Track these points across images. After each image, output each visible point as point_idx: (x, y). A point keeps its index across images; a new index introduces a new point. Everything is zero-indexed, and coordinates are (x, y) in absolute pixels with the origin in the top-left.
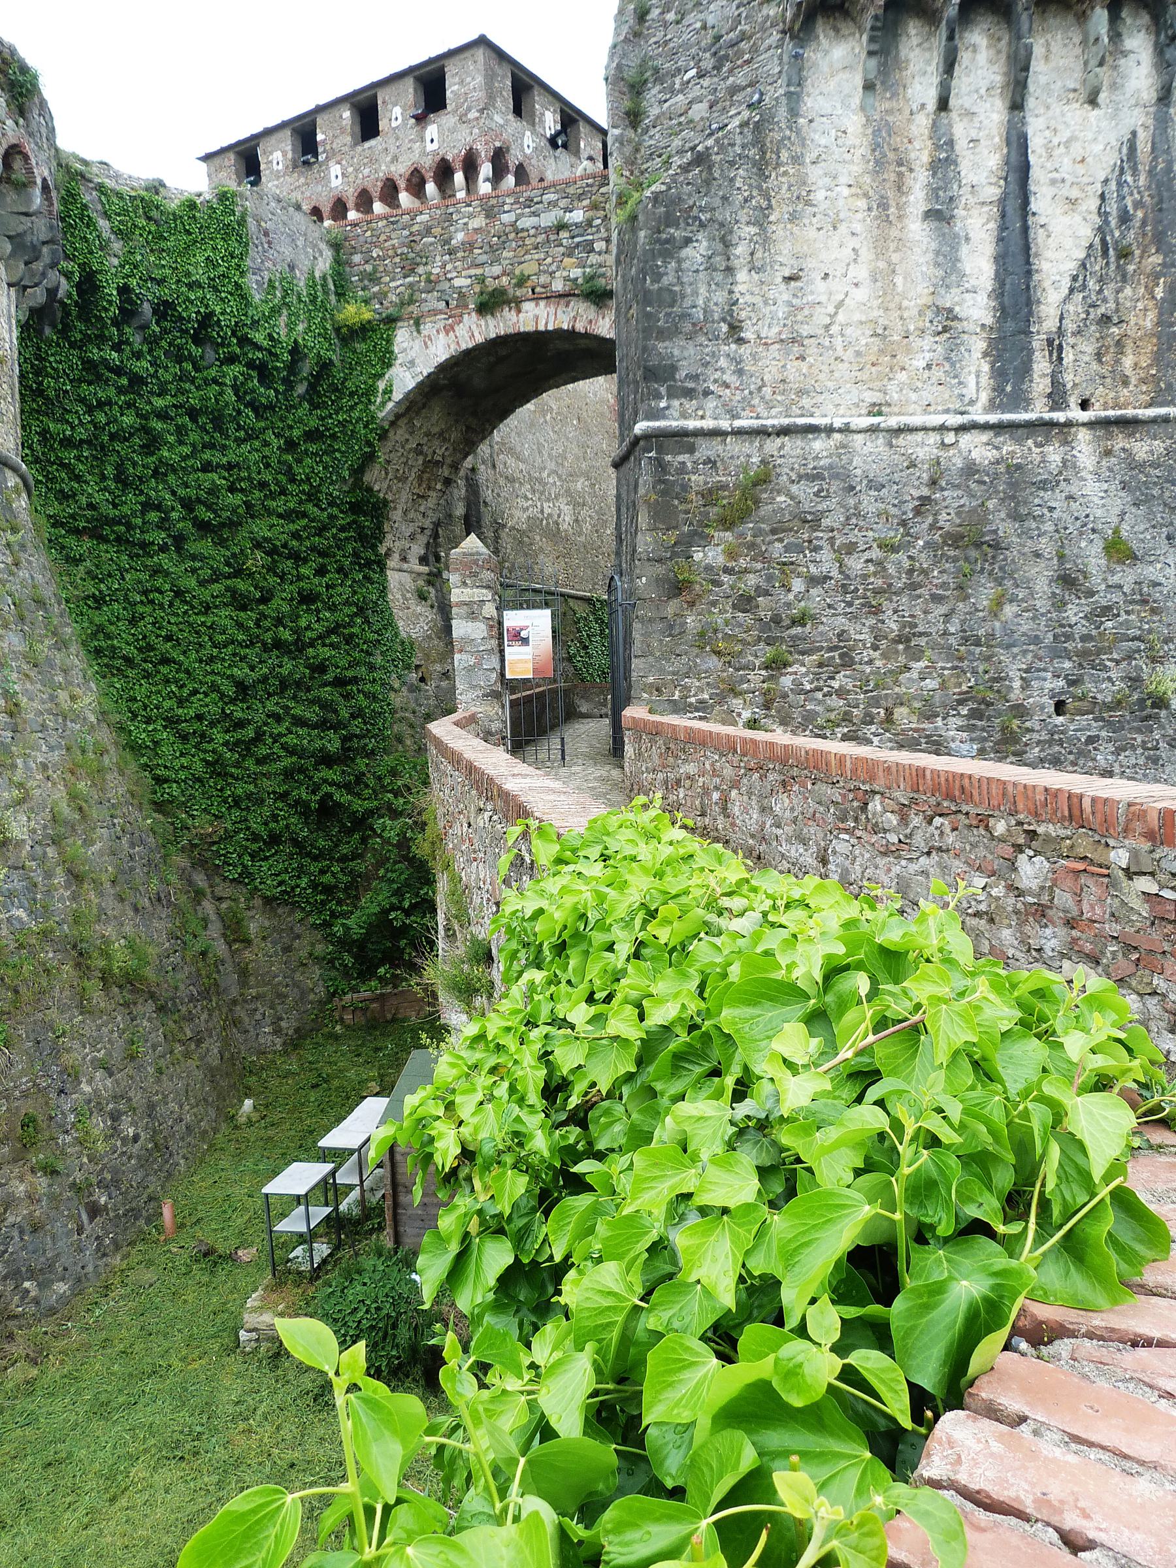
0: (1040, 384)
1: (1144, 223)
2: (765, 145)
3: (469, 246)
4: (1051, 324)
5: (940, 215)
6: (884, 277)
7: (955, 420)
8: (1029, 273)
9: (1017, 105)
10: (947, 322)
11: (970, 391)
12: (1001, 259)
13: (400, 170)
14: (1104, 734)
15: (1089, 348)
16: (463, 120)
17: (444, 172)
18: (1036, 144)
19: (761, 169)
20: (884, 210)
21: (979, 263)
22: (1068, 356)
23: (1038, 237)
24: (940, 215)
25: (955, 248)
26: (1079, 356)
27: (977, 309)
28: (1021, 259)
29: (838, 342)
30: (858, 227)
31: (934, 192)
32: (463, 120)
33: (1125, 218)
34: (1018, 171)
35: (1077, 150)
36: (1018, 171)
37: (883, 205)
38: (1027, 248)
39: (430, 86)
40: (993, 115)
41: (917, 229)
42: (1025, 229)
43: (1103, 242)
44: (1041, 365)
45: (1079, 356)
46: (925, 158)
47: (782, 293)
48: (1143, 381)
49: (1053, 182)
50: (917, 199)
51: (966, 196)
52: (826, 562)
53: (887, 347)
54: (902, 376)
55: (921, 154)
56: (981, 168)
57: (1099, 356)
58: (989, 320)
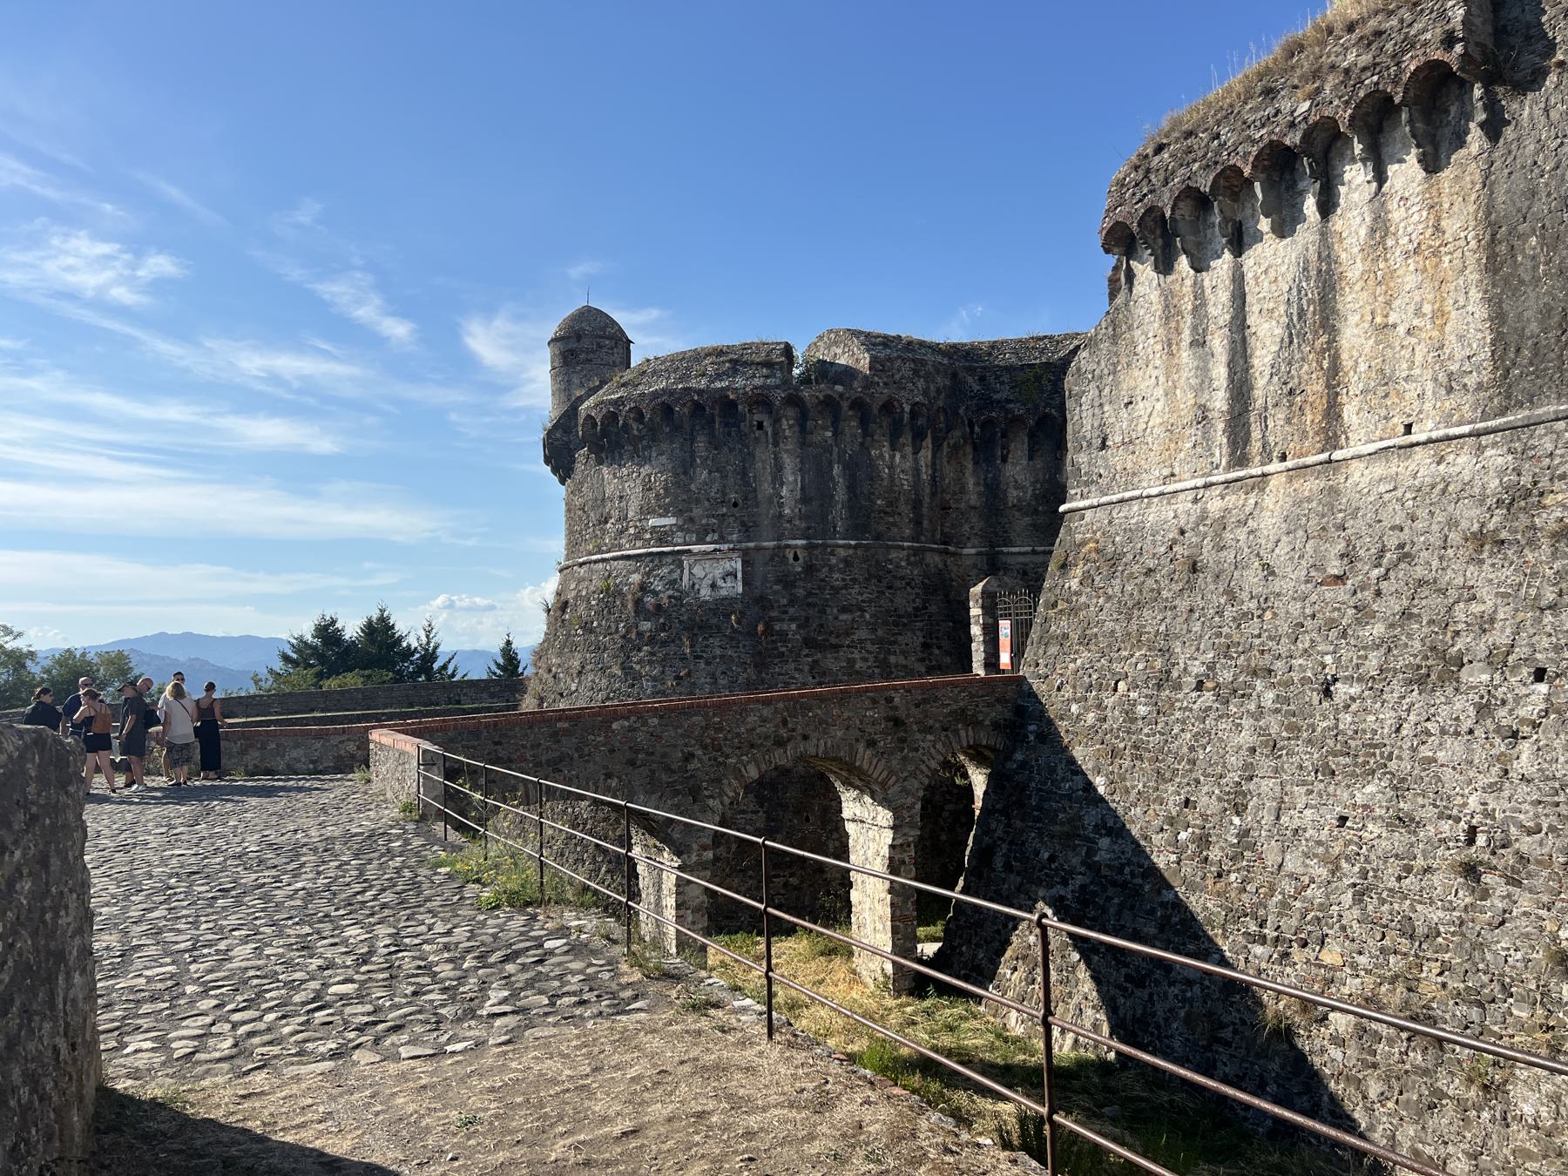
0: (1255, 446)
1: (1314, 313)
2: (1117, 326)
4: (1260, 402)
5: (1199, 343)
7: (1200, 482)
8: (1247, 367)
11: (1216, 460)
12: (1231, 365)
14: (1216, 705)
15: (1281, 415)
18: (1249, 276)
19: (1115, 339)
21: (1220, 372)
22: (1271, 424)
23: (1252, 341)
24: (1199, 343)
25: (1206, 362)
26: (1277, 419)
27: (1219, 401)
28: (1241, 362)
29: (1150, 440)
30: (1158, 363)
31: (1194, 328)
33: (1301, 314)
35: (1272, 274)
37: (1170, 345)
38: (1245, 350)
41: (1185, 356)
42: (1244, 340)
43: (1291, 335)
44: (1256, 434)
45: (1277, 419)
46: (1190, 307)
47: (1124, 413)
48: (1317, 433)
49: (1259, 300)
50: (1186, 336)
51: (1212, 327)
54: (1182, 455)
55: (1187, 305)
57: (1288, 421)
58: (1225, 408)
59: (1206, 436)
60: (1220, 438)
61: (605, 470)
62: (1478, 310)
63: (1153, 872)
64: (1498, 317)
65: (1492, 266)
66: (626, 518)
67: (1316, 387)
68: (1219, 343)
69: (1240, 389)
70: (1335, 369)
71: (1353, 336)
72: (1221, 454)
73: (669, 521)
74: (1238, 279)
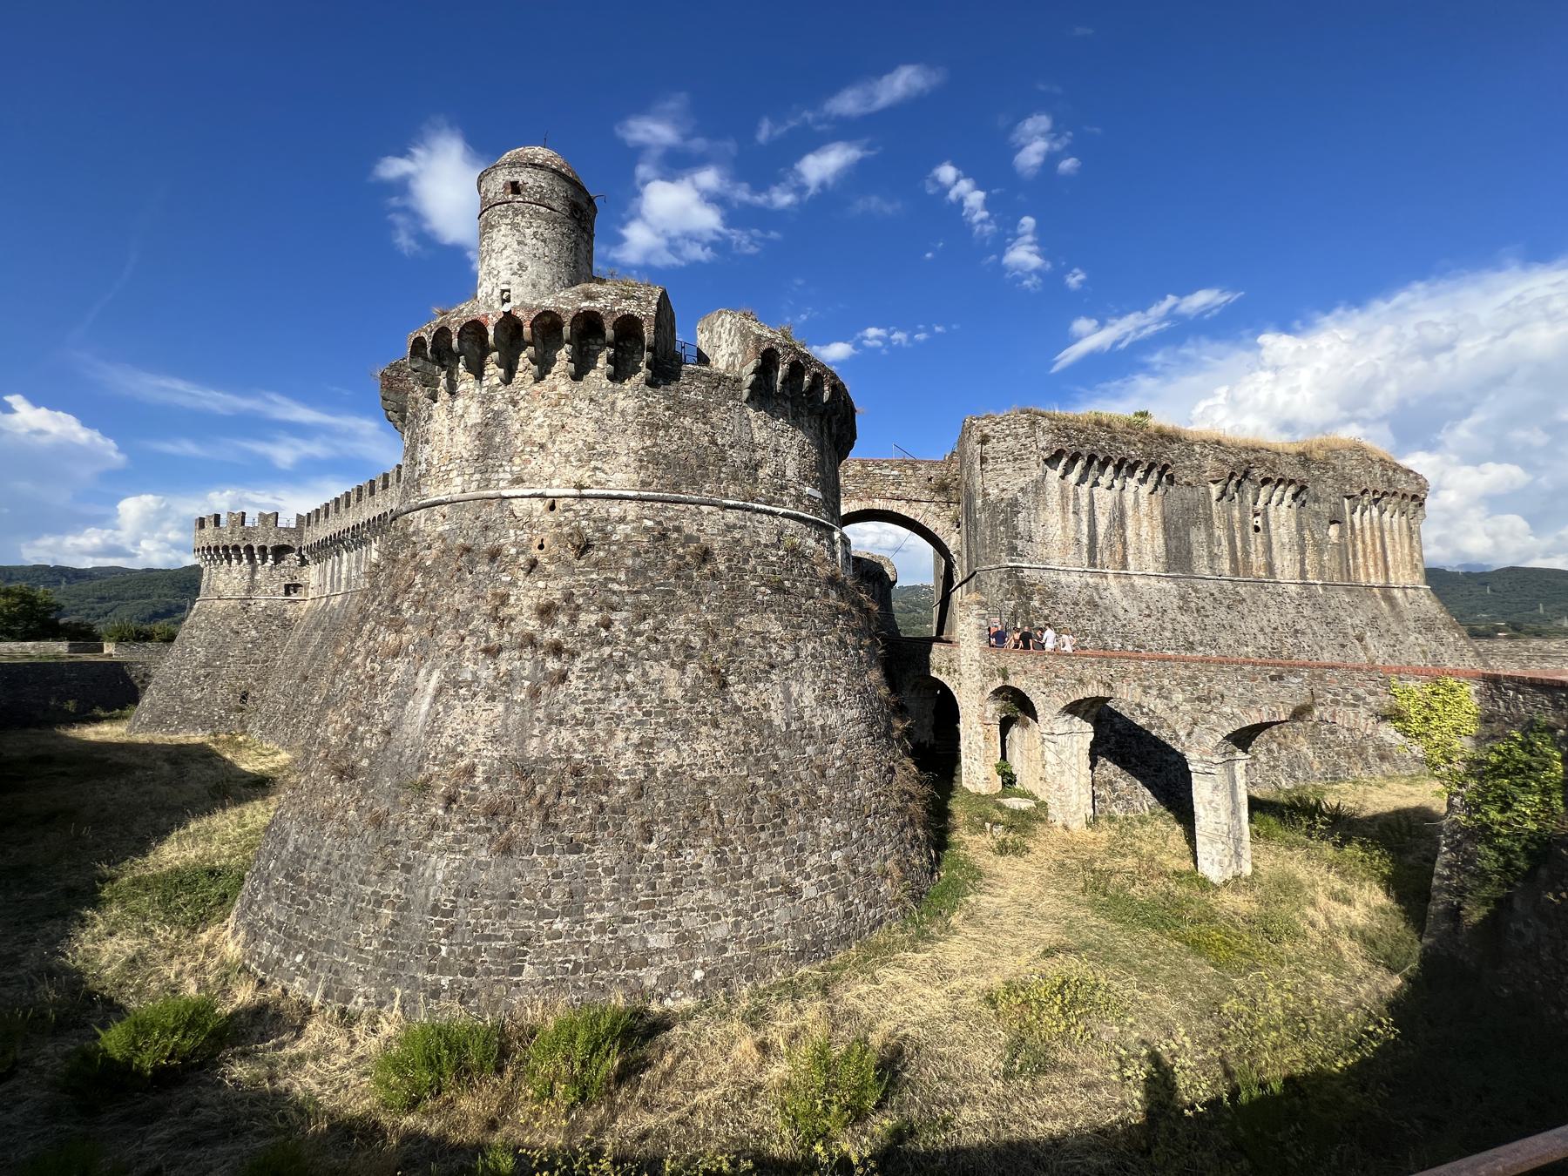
3: (855, 476)
6: (1064, 528)
20: (1064, 509)
21: (1085, 528)
27: (1085, 540)
34: (1092, 503)
36: (1092, 503)
41: (1071, 516)
45: (1107, 553)
52: (1061, 608)
53: (1065, 546)
56: (1084, 501)
59: (1080, 550)
61: (750, 412)
62: (1160, 541)
63: (1140, 728)
64: (1166, 544)
65: (1165, 530)
66: (784, 476)
67: (1118, 547)
68: (1084, 517)
69: (1093, 537)
70: (1124, 543)
71: (1130, 534)
72: (1085, 561)
73: (818, 494)
74: (1091, 496)
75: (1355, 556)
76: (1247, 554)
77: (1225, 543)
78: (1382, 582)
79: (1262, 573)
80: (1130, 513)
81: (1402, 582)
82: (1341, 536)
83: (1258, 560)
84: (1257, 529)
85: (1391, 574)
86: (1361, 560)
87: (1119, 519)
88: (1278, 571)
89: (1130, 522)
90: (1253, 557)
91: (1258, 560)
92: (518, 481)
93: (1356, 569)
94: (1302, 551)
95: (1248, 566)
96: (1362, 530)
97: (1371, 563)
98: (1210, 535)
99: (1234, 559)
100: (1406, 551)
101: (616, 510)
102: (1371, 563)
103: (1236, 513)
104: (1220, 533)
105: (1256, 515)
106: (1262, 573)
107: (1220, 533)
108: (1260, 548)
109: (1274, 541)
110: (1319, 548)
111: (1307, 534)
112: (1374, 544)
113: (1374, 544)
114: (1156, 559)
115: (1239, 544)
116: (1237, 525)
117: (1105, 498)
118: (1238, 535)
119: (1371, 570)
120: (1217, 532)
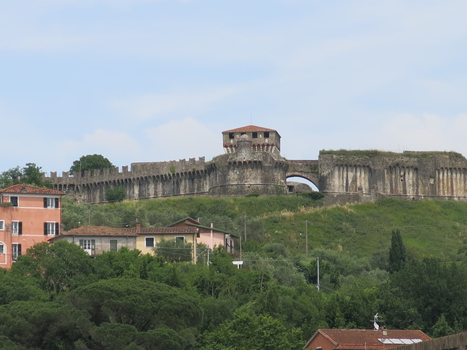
2: (332, 173)
5: (343, 179)
6: (339, 182)
9: (347, 172)
10: (343, 186)
13: (261, 143)
16: (272, 140)
17: (268, 145)
21: (345, 182)
24: (343, 179)
27: (345, 185)
32: (272, 140)
34: (347, 176)
36: (347, 176)
39: (266, 134)
40: (346, 172)
53: (339, 187)
56: (345, 176)
60: (345, 189)
67: (355, 186)
75: (439, 187)
76: (396, 187)
77: (389, 185)
78: (450, 195)
79: (401, 193)
80: (358, 178)
81: (459, 195)
82: (435, 182)
83: (400, 189)
84: (402, 180)
85: (455, 193)
86: (441, 188)
87: (355, 180)
88: (408, 192)
89: (358, 180)
90: (399, 188)
91: (400, 189)
92: (246, 182)
93: (439, 191)
94: (418, 186)
95: (396, 191)
96: (443, 179)
97: (446, 189)
98: (384, 183)
99: (392, 190)
100: (462, 185)
101: (259, 186)
102: (446, 189)
103: (394, 176)
104: (387, 182)
105: (401, 176)
106: (401, 193)
107: (387, 182)
108: (402, 186)
109: (407, 184)
110: (424, 186)
111: (420, 181)
112: (448, 183)
113: (448, 183)
114: (366, 190)
115: (394, 185)
116: (393, 180)
117: (351, 175)
118: (394, 182)
119: (446, 192)
120: (386, 182)
